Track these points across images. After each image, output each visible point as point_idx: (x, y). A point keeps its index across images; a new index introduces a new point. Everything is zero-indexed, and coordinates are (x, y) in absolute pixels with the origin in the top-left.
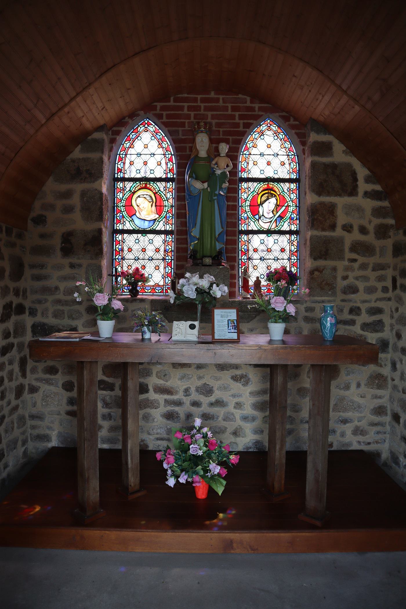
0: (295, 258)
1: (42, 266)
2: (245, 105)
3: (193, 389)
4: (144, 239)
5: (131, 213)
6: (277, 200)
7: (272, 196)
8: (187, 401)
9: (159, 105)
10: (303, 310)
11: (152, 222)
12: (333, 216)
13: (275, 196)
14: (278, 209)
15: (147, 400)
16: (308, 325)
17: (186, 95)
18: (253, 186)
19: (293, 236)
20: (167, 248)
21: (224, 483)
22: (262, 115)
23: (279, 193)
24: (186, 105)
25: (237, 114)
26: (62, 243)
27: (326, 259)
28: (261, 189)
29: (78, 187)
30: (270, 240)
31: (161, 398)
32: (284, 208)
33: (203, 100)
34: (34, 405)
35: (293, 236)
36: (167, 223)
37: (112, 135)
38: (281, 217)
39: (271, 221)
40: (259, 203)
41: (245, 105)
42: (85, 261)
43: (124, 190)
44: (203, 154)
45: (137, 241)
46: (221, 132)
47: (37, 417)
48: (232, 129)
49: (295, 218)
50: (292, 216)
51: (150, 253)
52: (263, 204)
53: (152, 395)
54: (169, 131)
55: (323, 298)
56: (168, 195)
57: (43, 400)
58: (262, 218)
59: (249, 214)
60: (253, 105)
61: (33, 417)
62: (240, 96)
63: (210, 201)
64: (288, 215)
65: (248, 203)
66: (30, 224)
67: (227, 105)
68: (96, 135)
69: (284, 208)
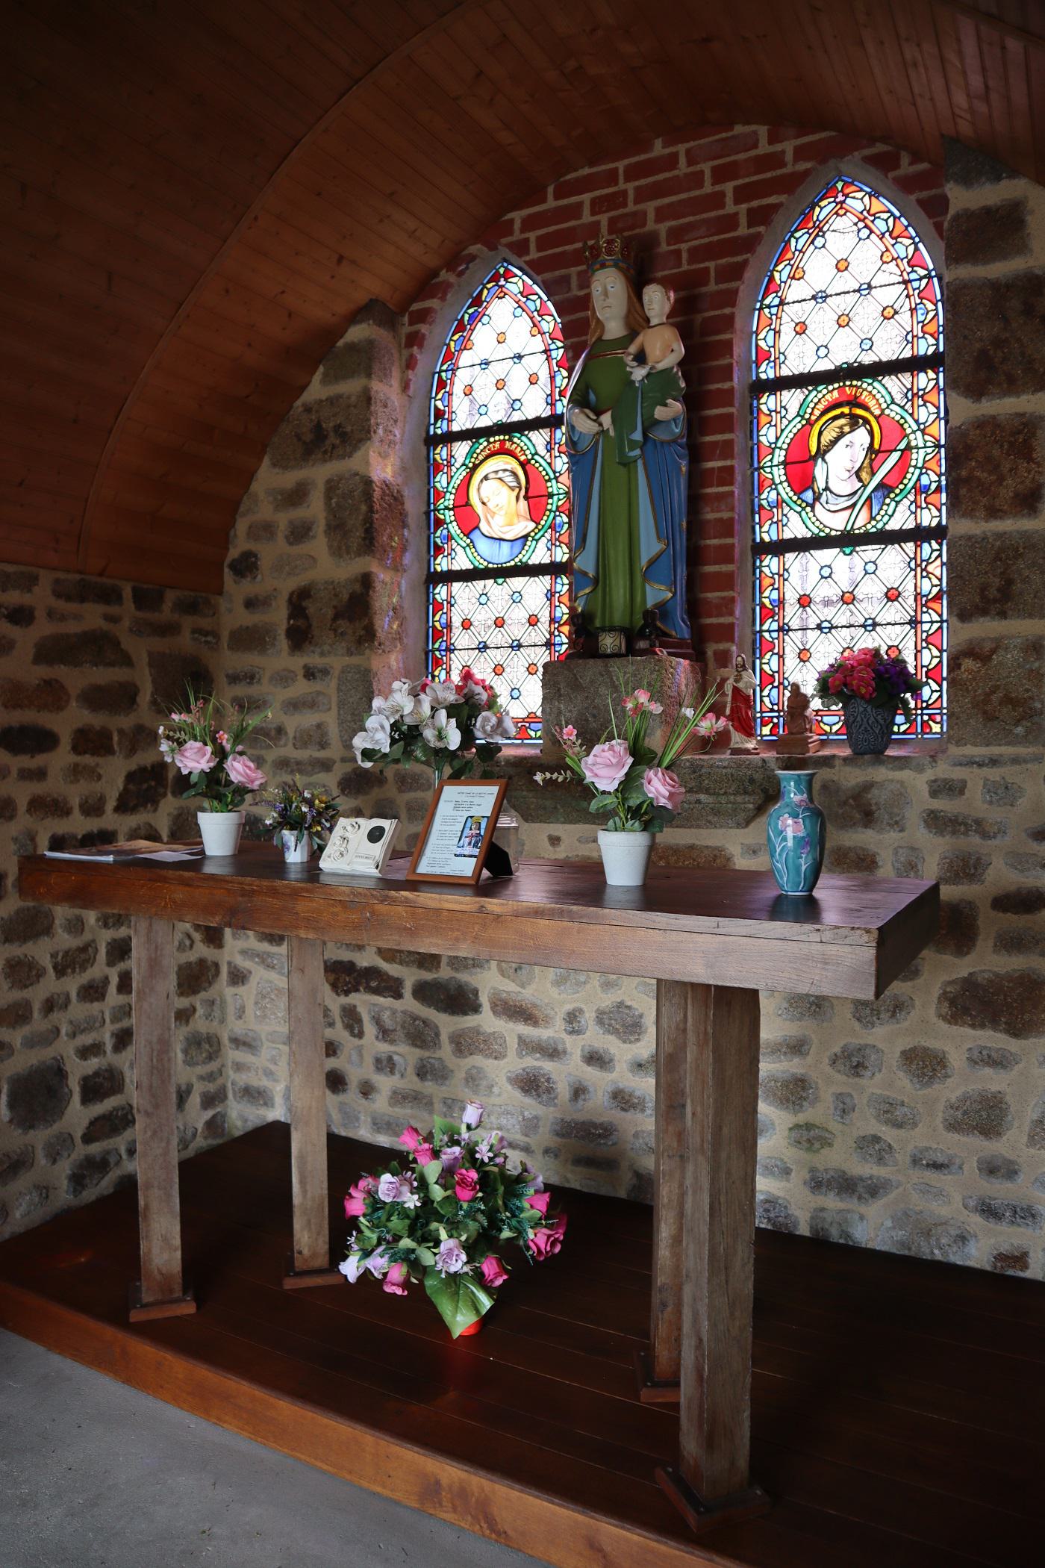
0: (936, 618)
1: (251, 678)
2: (753, 153)
3: (589, 1017)
4: (498, 591)
5: (470, 525)
6: (871, 433)
7: (855, 422)
8: (576, 1047)
9: (517, 216)
10: (924, 790)
11: (519, 543)
12: (1030, 459)
13: (866, 421)
14: (875, 464)
15: (476, 1031)
16: (940, 840)
17: (586, 171)
18: (792, 399)
19: (926, 546)
21: (486, 1302)
22: (806, 173)
23: (877, 412)
24: (586, 198)
25: (729, 187)
26: (290, 617)
27: (1003, 615)
28: (821, 407)
29: (320, 473)
30: (843, 565)
31: (511, 1030)
32: (896, 456)
33: (632, 174)
34: (241, 1013)
35: (926, 546)
36: (553, 543)
37: (411, 324)
38: (885, 488)
39: (854, 505)
40: (814, 450)
41: (753, 153)
42: (337, 661)
43: (450, 465)
44: (614, 329)
45: (483, 599)
46: (685, 256)
47: (245, 1044)
48: (716, 238)
49: (934, 486)
50: (925, 480)
51: (516, 629)
52: (826, 452)
53: (487, 1021)
55: (995, 750)
57: (256, 1003)
58: (823, 499)
59: (785, 491)
60: (778, 147)
61: (237, 1042)
62: (739, 129)
63: (624, 465)
64: (912, 476)
65: (780, 456)
66: (227, 573)
67: (698, 168)
68: (357, 333)
69: (896, 456)
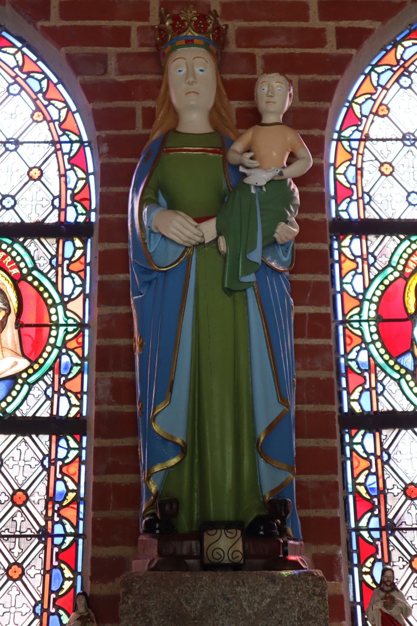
20: (60, 487)
36: (60, 389)
44: (195, 120)
48: (298, 51)
54: (69, 58)
56: (68, 286)
59: (377, 350)
63: (229, 291)
65: (369, 310)
